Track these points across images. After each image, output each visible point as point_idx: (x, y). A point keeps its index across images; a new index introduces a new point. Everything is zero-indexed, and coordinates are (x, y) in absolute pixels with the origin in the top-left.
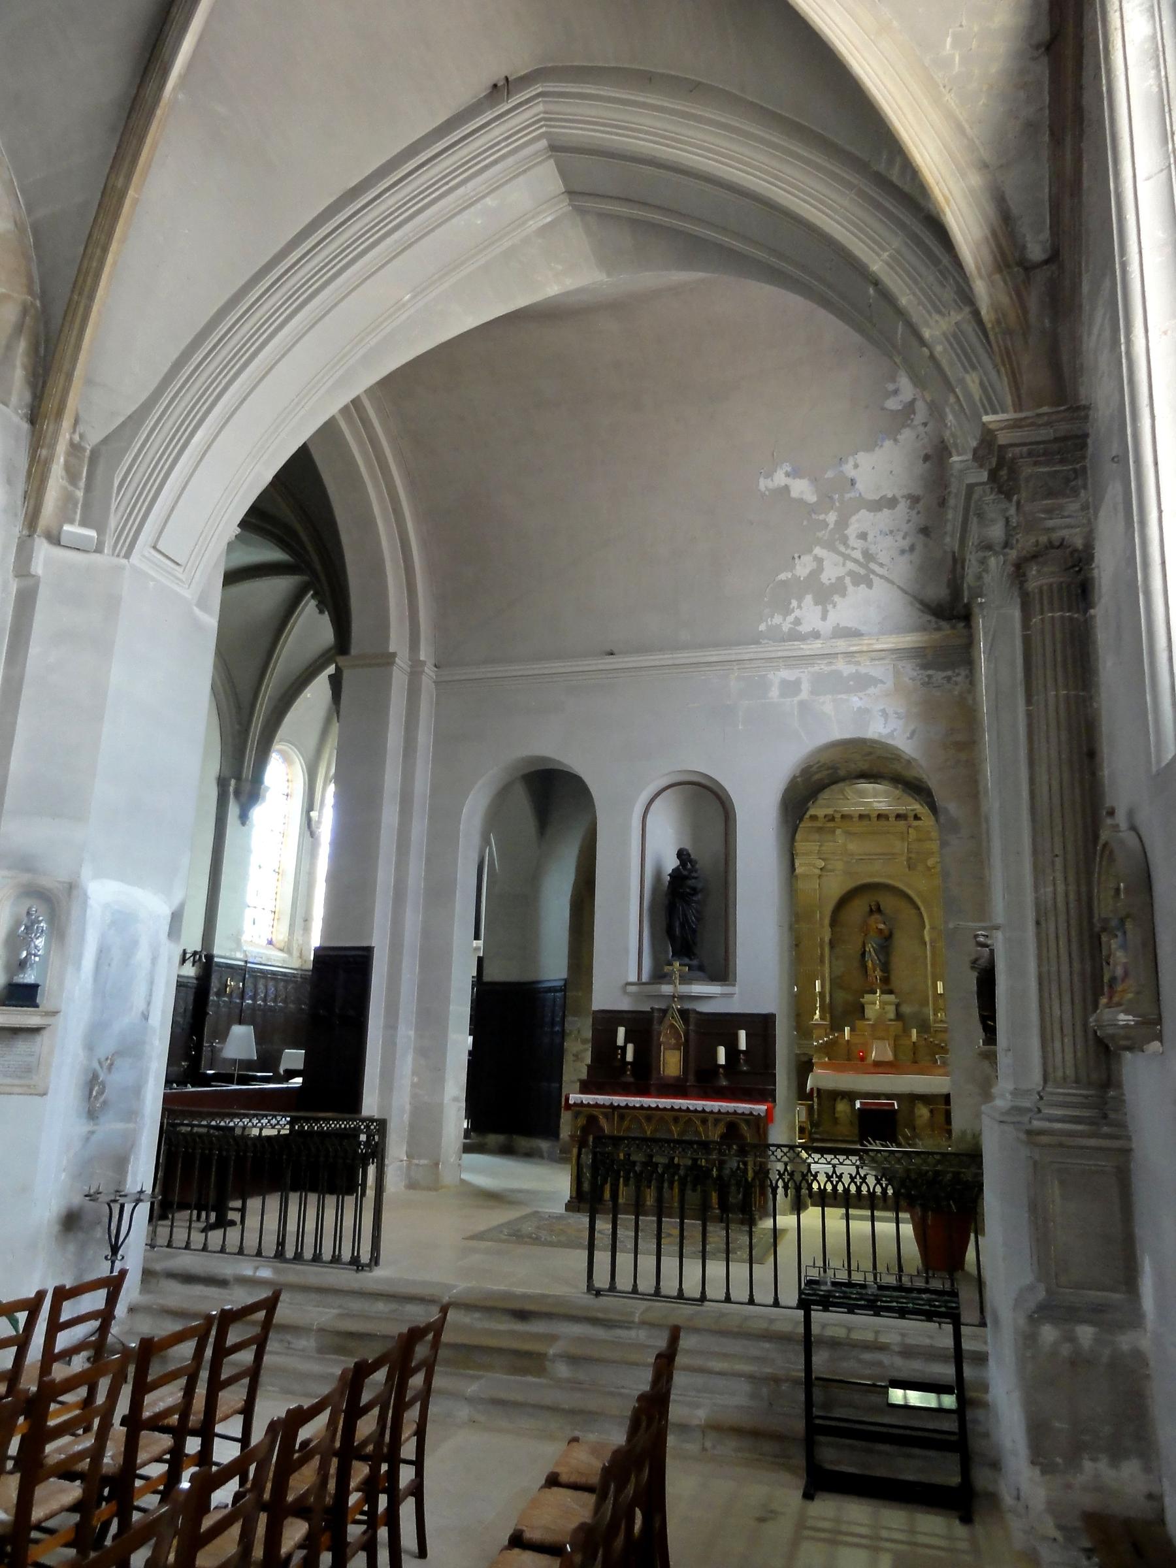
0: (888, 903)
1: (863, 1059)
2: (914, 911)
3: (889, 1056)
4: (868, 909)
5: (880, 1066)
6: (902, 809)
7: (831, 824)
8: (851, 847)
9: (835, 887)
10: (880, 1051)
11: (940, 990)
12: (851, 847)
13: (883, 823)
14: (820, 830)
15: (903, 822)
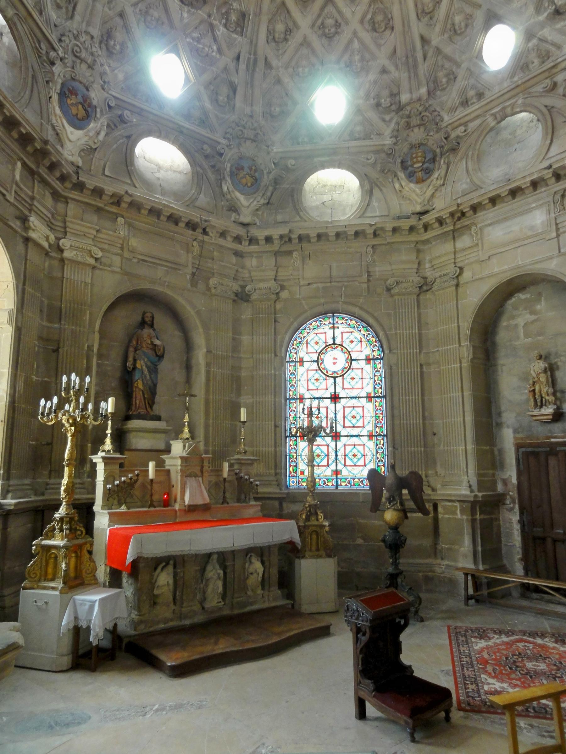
0: (162, 321)
1: (166, 503)
2: (178, 333)
3: (204, 498)
4: (140, 318)
5: (197, 514)
6: (195, 217)
7: (114, 209)
8: (134, 242)
9: (109, 285)
10: (189, 494)
11: (243, 418)
12: (134, 242)
13: (172, 226)
14: (99, 210)
15: (190, 232)
